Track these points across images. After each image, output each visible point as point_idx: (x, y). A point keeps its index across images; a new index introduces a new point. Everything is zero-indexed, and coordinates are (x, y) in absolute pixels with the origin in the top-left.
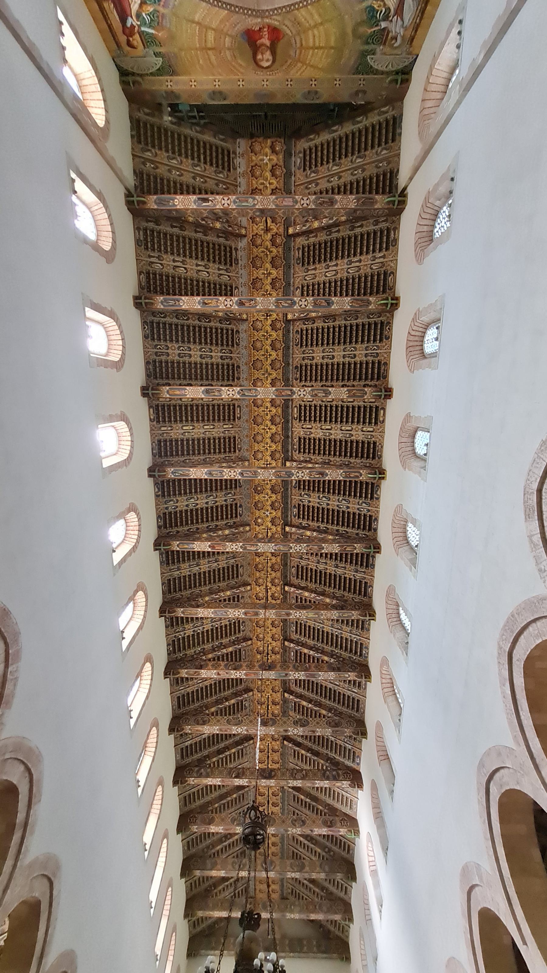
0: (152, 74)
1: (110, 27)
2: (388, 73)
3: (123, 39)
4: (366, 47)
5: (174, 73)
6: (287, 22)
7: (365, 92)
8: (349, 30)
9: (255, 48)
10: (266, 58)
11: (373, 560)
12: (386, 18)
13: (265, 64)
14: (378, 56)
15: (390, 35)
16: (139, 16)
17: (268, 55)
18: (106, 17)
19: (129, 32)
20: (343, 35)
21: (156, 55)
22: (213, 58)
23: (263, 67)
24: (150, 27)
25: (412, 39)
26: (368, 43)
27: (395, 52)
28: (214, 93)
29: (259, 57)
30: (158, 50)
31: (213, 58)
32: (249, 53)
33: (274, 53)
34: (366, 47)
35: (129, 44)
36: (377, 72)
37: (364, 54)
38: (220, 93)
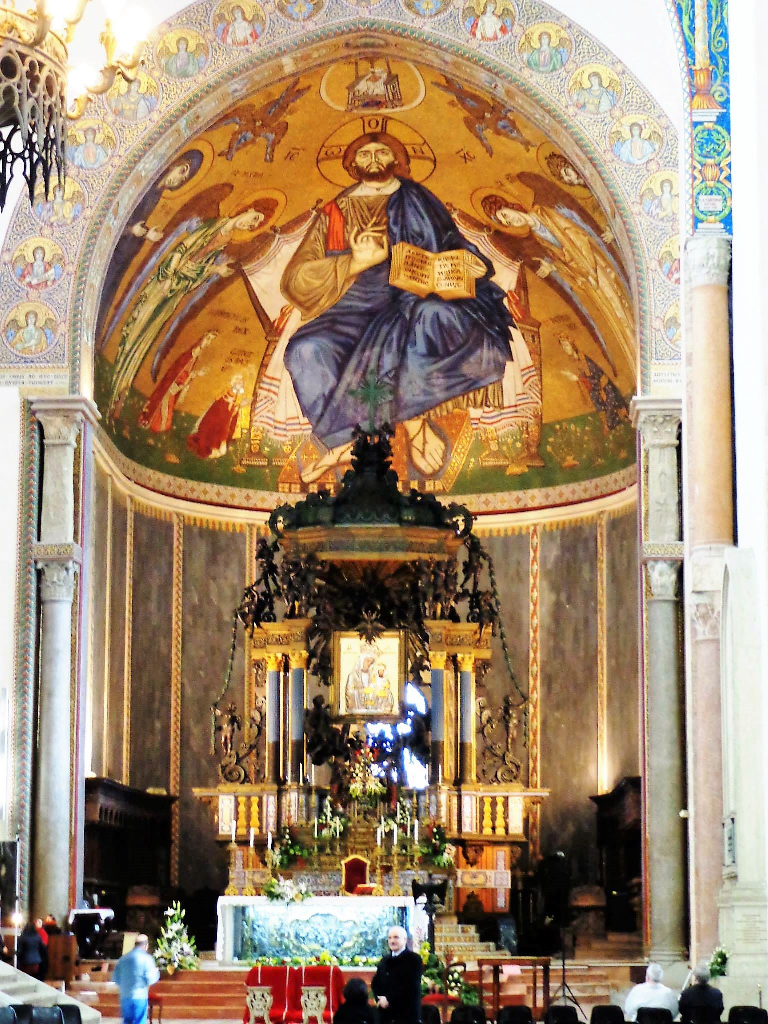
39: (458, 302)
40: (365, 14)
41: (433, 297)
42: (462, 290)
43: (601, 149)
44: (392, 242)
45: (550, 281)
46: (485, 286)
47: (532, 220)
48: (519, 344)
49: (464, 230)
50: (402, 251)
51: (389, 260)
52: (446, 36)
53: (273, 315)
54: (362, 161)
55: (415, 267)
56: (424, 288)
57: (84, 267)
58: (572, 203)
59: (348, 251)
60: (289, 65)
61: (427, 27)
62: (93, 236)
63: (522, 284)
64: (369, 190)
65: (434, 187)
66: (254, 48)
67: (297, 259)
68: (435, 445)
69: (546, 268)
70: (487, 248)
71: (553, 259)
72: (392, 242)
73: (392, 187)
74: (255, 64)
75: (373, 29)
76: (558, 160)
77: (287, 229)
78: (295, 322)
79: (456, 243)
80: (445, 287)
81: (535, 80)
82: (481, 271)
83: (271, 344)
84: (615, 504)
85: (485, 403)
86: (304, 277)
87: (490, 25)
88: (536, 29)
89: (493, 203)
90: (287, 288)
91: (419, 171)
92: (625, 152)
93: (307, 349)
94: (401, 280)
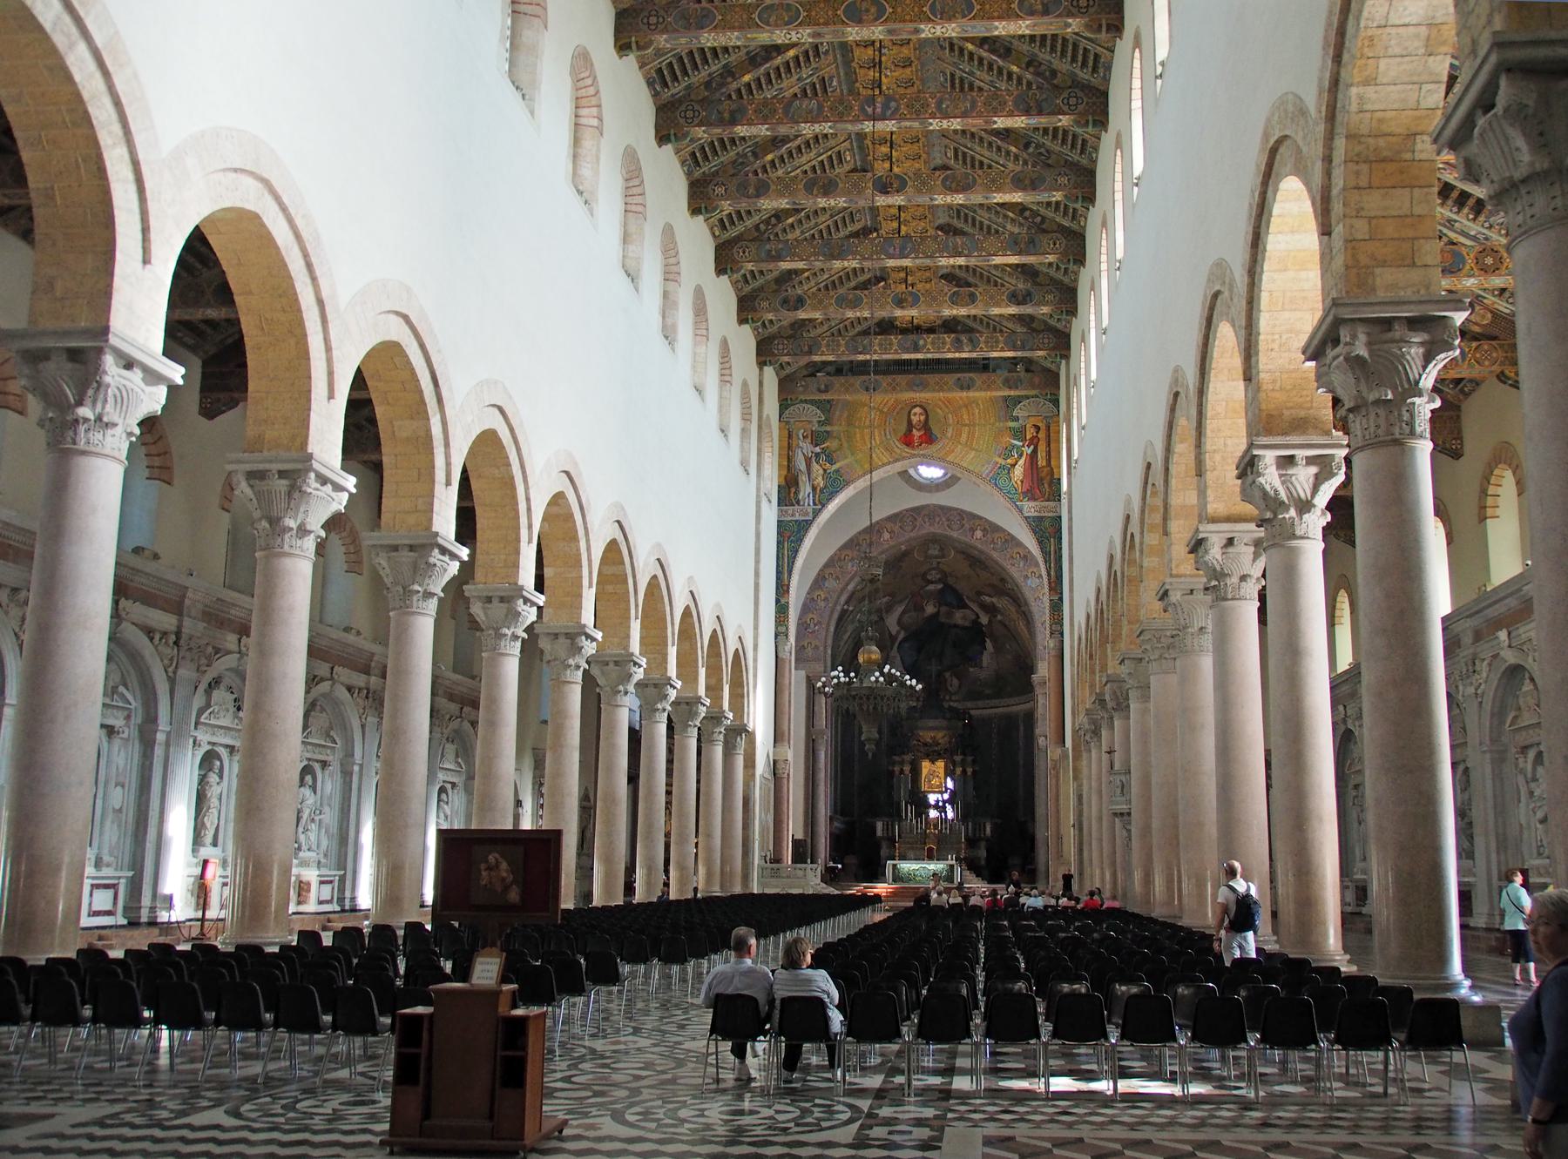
0: (1027, 397)
1: (1049, 445)
2: (801, 401)
3: (1042, 435)
4: (828, 428)
5: (1006, 399)
6: (898, 451)
7: (820, 391)
8: (845, 445)
9: (926, 426)
10: (917, 417)
11: (655, 89)
12: (817, 455)
13: (917, 410)
14: (815, 420)
15: (809, 440)
16: (1021, 455)
17: (915, 419)
18: (1049, 454)
19: (1034, 441)
20: (850, 438)
21: (1017, 419)
22: (965, 417)
23: (921, 406)
24: (1014, 446)
25: (790, 436)
26: (827, 432)
27: (800, 424)
28: (969, 388)
29: (922, 418)
30: (1012, 424)
31: (965, 417)
32: (930, 422)
33: (910, 421)
34: (828, 428)
35: (1038, 428)
36: (812, 402)
37: (827, 422)
38: (962, 388)
39: (964, 628)
40: (932, 530)
41: (955, 626)
42: (967, 624)
43: (1020, 580)
44: (940, 605)
45: (1000, 622)
46: (976, 622)
47: (994, 600)
48: (989, 644)
49: (970, 604)
50: (944, 609)
51: (938, 612)
52: (963, 538)
53: (894, 633)
54: (929, 577)
55: (950, 615)
56: (953, 622)
57: (828, 625)
58: (1008, 595)
59: (923, 609)
60: (903, 547)
61: (955, 535)
62: (832, 612)
63: (990, 621)
64: (931, 587)
65: (958, 587)
66: (892, 543)
67: (904, 612)
68: (956, 682)
69: (999, 617)
70: (976, 609)
71: (1002, 614)
72: (940, 605)
73: (940, 586)
74: (892, 547)
75: (934, 534)
76: (1003, 580)
77: (901, 601)
78: (902, 635)
79: (965, 606)
80: (960, 622)
81: (995, 555)
82: (974, 617)
83: (893, 644)
84: (1027, 706)
85: (976, 666)
86: (906, 619)
87: (979, 534)
88: (996, 535)
89: (979, 593)
90: (899, 622)
91: (951, 581)
92: (1029, 582)
93: (906, 645)
94: (943, 619)
